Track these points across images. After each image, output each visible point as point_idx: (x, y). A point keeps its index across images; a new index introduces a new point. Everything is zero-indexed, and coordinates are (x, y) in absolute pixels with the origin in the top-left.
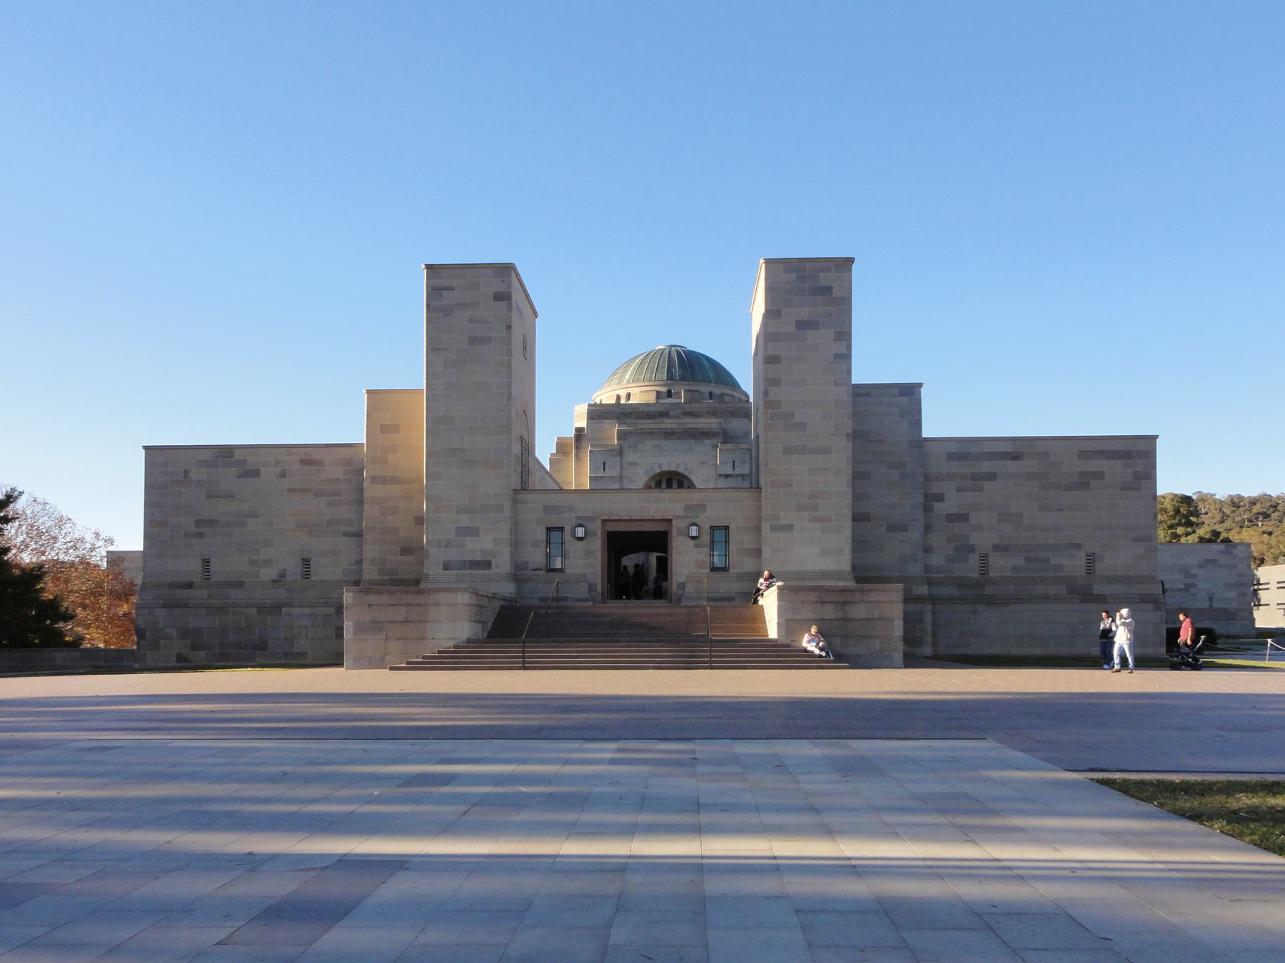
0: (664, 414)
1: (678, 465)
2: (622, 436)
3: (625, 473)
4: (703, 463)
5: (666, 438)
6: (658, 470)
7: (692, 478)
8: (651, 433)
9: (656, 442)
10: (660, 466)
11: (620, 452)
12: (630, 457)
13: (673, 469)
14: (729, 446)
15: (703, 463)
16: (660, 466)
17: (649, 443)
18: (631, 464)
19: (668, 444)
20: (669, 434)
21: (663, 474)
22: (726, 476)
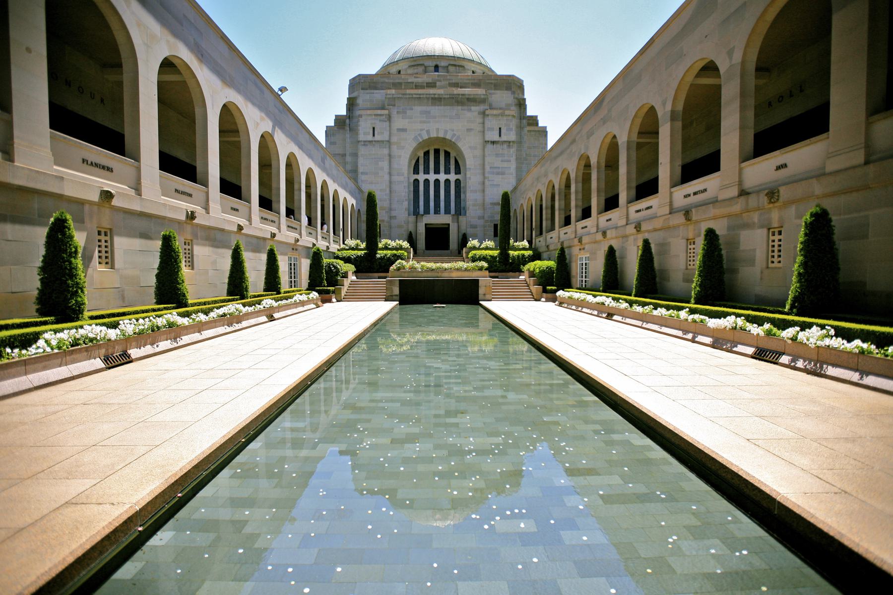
0: (431, 85)
1: (446, 132)
2: (392, 101)
3: (394, 139)
4: (469, 130)
5: (433, 104)
6: (426, 137)
7: (460, 145)
8: (419, 98)
9: (424, 108)
10: (428, 132)
11: (389, 118)
12: (399, 122)
13: (441, 135)
14: (495, 112)
15: (469, 130)
16: (428, 132)
17: (418, 109)
18: (399, 130)
19: (435, 110)
20: (437, 100)
21: (431, 141)
22: (493, 143)
